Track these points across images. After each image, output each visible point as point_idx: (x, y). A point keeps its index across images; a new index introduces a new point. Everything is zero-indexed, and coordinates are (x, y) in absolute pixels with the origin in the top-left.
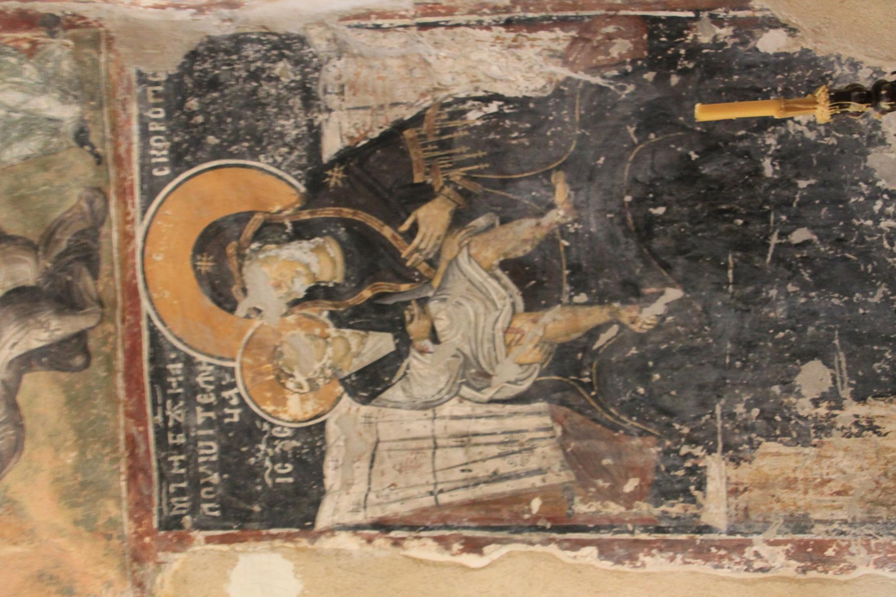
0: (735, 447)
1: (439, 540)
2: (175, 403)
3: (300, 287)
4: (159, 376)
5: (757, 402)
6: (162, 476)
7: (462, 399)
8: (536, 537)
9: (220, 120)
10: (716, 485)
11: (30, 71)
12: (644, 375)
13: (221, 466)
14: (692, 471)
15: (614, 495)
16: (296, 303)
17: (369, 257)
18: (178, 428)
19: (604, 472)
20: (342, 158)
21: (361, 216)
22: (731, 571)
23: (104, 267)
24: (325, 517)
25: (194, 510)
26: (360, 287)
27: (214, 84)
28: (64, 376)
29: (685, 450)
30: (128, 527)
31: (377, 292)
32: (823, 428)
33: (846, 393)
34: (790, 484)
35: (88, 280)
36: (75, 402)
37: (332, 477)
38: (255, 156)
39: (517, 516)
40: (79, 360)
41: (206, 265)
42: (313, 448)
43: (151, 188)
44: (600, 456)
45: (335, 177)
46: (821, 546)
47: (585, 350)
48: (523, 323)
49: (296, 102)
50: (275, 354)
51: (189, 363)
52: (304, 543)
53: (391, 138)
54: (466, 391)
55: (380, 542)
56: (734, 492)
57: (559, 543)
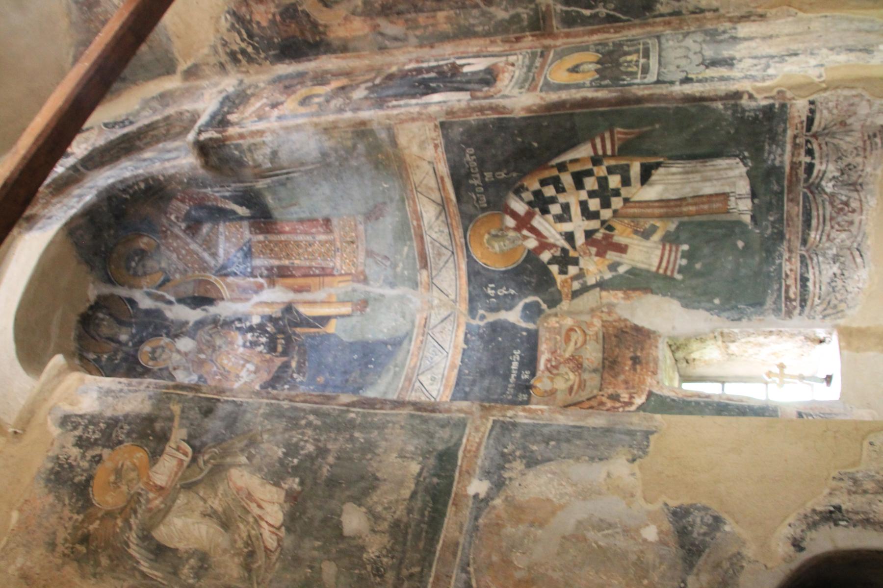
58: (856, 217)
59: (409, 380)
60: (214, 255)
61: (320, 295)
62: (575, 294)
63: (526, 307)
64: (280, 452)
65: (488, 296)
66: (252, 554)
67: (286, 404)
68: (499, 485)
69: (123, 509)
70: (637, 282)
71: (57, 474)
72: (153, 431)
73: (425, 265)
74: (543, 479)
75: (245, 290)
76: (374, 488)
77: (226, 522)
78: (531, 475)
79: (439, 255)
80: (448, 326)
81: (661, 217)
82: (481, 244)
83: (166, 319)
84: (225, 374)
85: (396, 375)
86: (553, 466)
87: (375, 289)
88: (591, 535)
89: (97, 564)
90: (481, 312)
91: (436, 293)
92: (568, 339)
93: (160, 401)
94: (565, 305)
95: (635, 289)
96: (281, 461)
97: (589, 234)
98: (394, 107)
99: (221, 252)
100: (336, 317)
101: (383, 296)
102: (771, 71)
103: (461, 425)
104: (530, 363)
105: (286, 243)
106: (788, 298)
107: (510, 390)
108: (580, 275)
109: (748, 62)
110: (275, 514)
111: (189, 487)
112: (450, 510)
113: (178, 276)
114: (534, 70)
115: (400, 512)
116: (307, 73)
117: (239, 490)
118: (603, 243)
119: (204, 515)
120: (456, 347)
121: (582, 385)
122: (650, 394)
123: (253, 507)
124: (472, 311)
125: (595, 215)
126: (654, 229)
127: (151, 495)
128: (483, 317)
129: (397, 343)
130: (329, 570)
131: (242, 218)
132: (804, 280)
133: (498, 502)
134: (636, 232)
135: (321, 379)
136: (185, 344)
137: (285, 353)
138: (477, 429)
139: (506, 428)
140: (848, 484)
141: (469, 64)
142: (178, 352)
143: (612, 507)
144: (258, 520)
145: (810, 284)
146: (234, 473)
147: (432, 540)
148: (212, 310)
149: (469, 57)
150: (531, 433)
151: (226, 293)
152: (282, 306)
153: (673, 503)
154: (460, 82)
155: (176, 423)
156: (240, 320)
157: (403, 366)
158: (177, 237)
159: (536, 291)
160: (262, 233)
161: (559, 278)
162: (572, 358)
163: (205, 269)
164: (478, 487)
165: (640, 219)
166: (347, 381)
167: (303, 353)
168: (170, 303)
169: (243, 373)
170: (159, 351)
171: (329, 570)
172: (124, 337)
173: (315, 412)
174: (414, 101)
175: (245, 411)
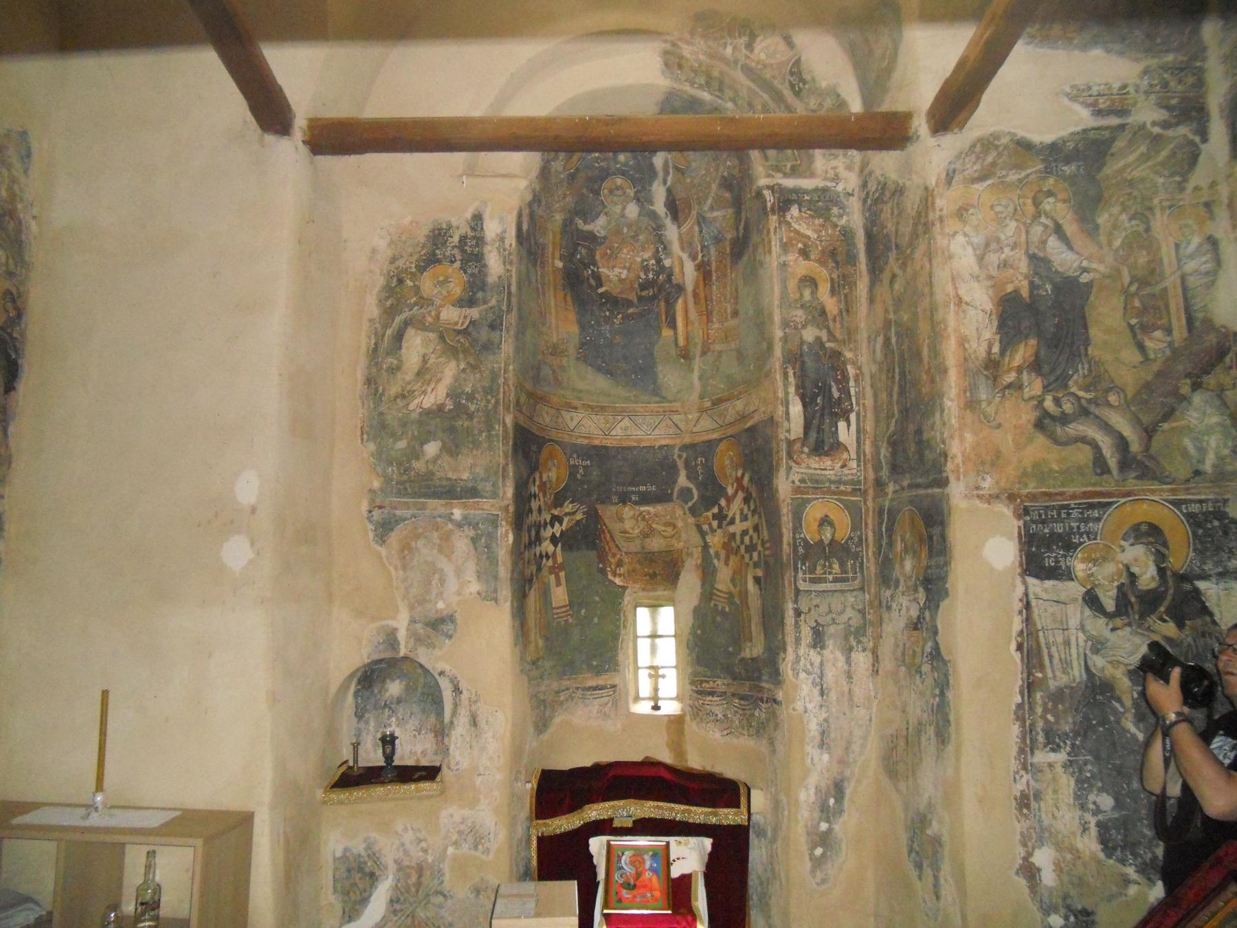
0: (1071, 765)
1: (1022, 631)
2: (1082, 513)
3: (1135, 570)
4: (1091, 506)
5: (1093, 776)
6: (1047, 507)
7: (1086, 642)
8: (1025, 675)
9: (1209, 536)
10: (1053, 757)
11: (1226, 452)
12: (1103, 725)
13: (1052, 534)
14: (1059, 746)
15: (1046, 711)
16: (1127, 568)
17: (1150, 602)
18: (1069, 514)
19: (1055, 706)
20: (1197, 591)
21: (1169, 598)
22: (1014, 765)
23: (1140, 482)
24: (1031, 581)
25: (1033, 521)
26: (1137, 597)
27: (1226, 533)
28: (1091, 464)
29: (1068, 742)
30: (1025, 492)
31: (1133, 604)
32: (1083, 807)
33: (1100, 817)
34: (1055, 792)
35: (1134, 475)
36: (1080, 470)
37: (1049, 583)
38: (1195, 550)
39: (1034, 667)
40: (1099, 471)
41: (1144, 528)
42: (1062, 575)
43: (1177, 504)
44: (1062, 702)
45: (1188, 587)
46: (1028, 806)
47: (1112, 697)
48: (1122, 669)
49: (1221, 570)
50: (1105, 559)
51: (1099, 519)
52: (1019, 570)
53: (1205, 611)
54: (1090, 643)
55: (1020, 604)
56: (1050, 765)
57: (1022, 686)
58: (745, 732)
60: (712, 209)
61: (693, 315)
62: (699, 527)
63: (689, 490)
64: (468, 390)
65: (696, 458)
66: (403, 397)
68: (459, 525)
69: (422, 298)
70: (707, 572)
71: (440, 234)
72: (474, 294)
73: (714, 404)
74: (464, 548)
76: (452, 456)
78: (466, 541)
79: (720, 416)
81: (740, 592)
82: (728, 450)
83: (651, 185)
84: (612, 257)
85: (627, 399)
86: (473, 551)
87: (697, 363)
88: (437, 576)
89: (387, 298)
91: (697, 415)
92: (667, 524)
93: (498, 286)
94: (691, 520)
95: (704, 572)
96: (463, 392)
97: (733, 535)
99: (715, 214)
101: (693, 371)
102: (803, 675)
103: (494, 495)
104: (645, 499)
105: (725, 275)
106: (702, 682)
107: (620, 489)
108: (713, 531)
109: (817, 660)
110: (429, 401)
111: (442, 337)
112: (442, 502)
113: (689, 180)
114: (833, 487)
115: (439, 474)
116: (855, 265)
117: (442, 372)
118: (729, 547)
120: (655, 440)
121: (629, 540)
124: (685, 448)
125: (742, 542)
126: (735, 586)
127: (433, 313)
128: (680, 456)
129: (656, 392)
130: (402, 444)
131: (737, 229)
132: (712, 694)
133: (450, 526)
134: (734, 572)
135: (618, 339)
136: (632, 210)
137: (640, 298)
138: (493, 506)
139: (494, 522)
140: (474, 698)
141: (849, 426)
142: (624, 208)
143: (452, 585)
144: (425, 392)
145: (710, 698)
146: (453, 364)
147: (426, 496)
148: (668, 222)
150: (491, 536)
151: (684, 229)
152: (681, 282)
153: (457, 616)
154: (821, 422)
156: (665, 248)
157: (637, 402)
158: (717, 170)
160: (732, 249)
161: (710, 514)
162: (652, 530)
163: (699, 203)
164: (457, 514)
165: (737, 577)
166: (618, 361)
167: (641, 315)
168: (665, 182)
169: (617, 270)
170: (619, 192)
171: (402, 444)
173: (497, 403)
174: (792, 390)
175: (494, 354)
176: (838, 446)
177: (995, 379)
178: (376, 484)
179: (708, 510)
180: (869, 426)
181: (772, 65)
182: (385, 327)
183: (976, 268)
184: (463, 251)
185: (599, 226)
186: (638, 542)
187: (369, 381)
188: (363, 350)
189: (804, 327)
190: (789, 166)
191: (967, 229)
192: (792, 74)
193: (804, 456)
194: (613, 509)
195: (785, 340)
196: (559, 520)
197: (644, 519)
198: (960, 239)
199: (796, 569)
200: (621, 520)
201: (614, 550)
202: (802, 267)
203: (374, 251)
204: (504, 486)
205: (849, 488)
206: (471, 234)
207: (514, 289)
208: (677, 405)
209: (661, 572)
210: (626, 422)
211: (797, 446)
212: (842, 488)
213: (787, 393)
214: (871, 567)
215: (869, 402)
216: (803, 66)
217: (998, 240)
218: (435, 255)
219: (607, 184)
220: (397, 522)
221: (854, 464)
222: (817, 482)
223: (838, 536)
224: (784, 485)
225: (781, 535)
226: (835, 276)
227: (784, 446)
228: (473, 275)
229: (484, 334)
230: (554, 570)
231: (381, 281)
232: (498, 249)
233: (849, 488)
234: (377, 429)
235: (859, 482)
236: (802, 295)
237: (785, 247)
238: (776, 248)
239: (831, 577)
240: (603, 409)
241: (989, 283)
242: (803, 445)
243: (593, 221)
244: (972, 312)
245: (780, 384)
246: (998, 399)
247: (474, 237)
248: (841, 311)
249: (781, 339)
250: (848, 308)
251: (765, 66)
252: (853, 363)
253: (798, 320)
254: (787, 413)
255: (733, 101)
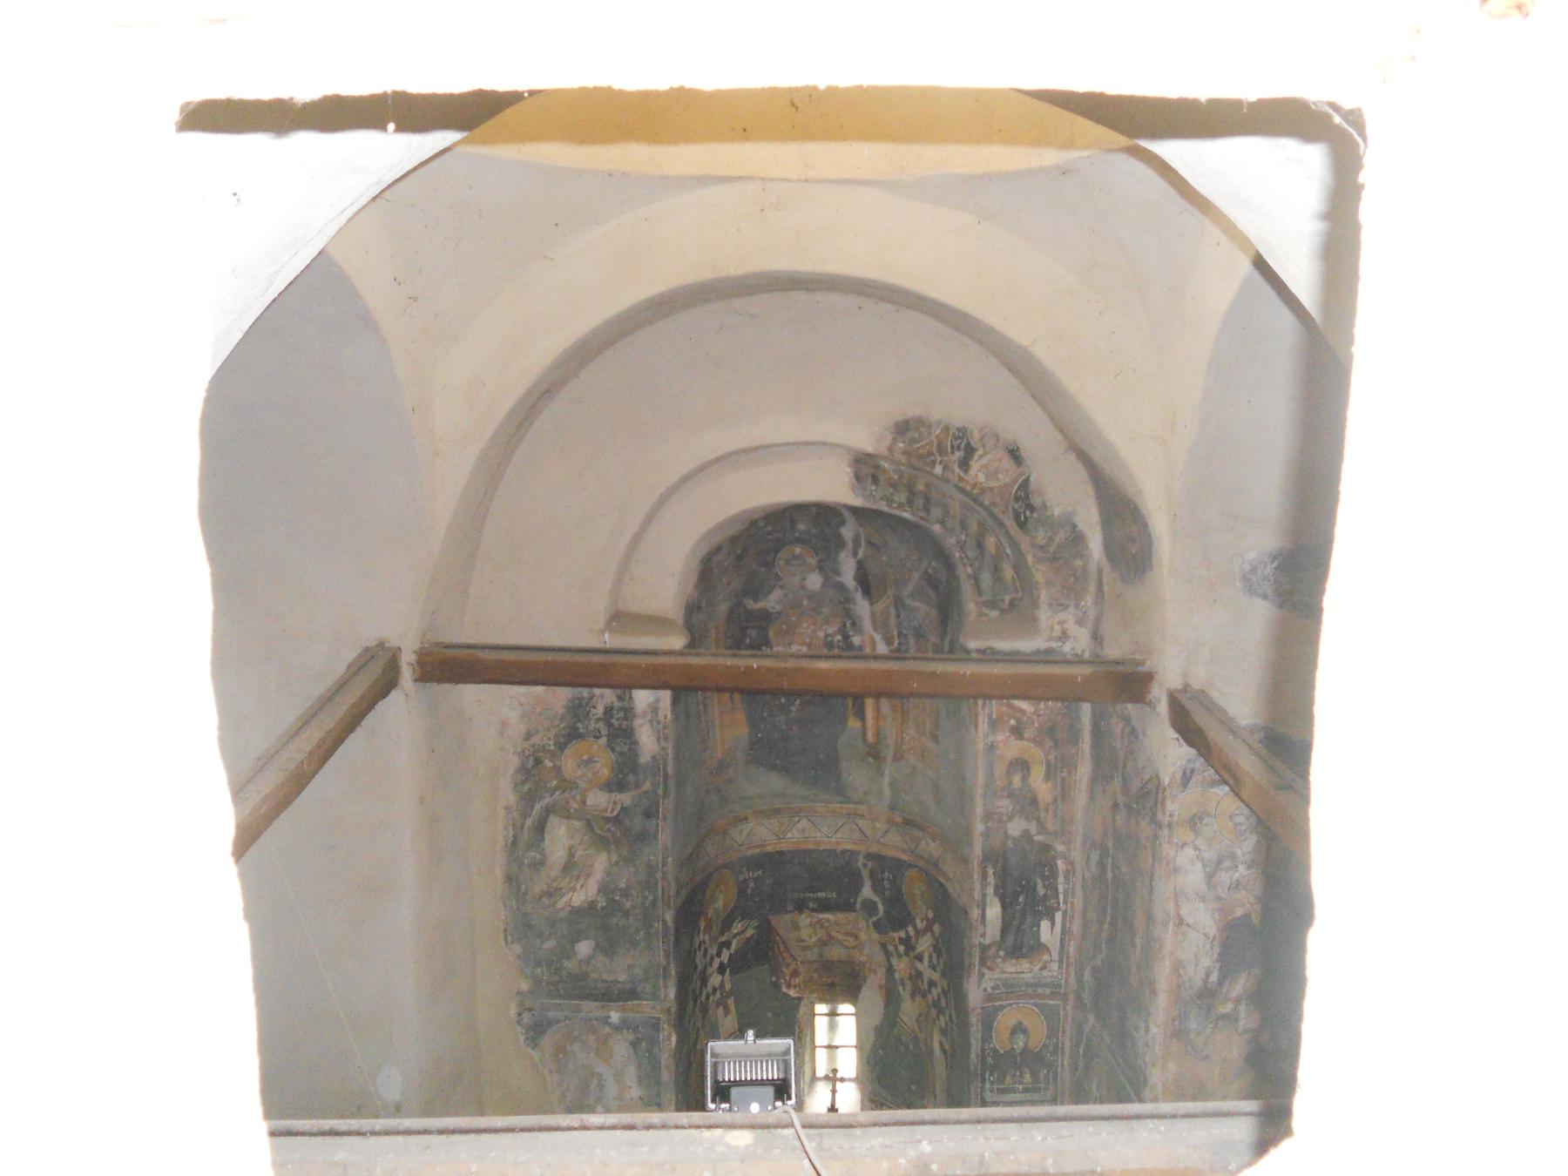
59: (801, 810)
62: (884, 946)
63: (874, 903)
64: (622, 885)
67: (659, 875)
68: (617, 1028)
70: (891, 999)
75: (885, 624)
77: (569, 867)
80: (857, 835)
83: (837, 554)
87: (889, 769)
88: (595, 1081)
89: (524, 782)
90: (870, 864)
92: (847, 934)
94: (875, 936)
98: (984, 875)
100: (864, 726)
103: (655, 997)
104: (825, 906)
110: (578, 899)
111: (589, 824)
115: (593, 976)
119: (570, 848)
121: (806, 948)
122: (800, 999)
123: (582, 881)
124: (869, 856)
128: (865, 866)
129: (840, 791)
130: (550, 944)
136: (814, 581)
139: (655, 1025)
144: (574, 890)
146: (603, 857)
147: (580, 997)
148: (859, 596)
149: (1063, 924)
150: (653, 1042)
151: (881, 605)
154: (1022, 923)
155: (634, 793)
156: (854, 624)
159: (887, 913)
164: (615, 1017)
168: (855, 554)
171: (550, 944)
172: (801, 527)
174: (990, 890)
176: (1039, 947)
177: (1209, 1009)
178: (525, 986)
179: (894, 930)
180: (1076, 928)
181: (991, 489)
182: (524, 816)
183: (1204, 887)
184: (610, 725)
185: (773, 601)
186: (816, 950)
187: (509, 879)
188: (501, 843)
189: (1010, 819)
190: (1007, 599)
191: (1197, 842)
192: (1017, 499)
193: (999, 960)
194: (788, 917)
195: (986, 835)
196: (727, 944)
197: (822, 926)
198: (1190, 852)
199: (983, 1080)
200: (797, 928)
201: (789, 960)
202: (1012, 748)
203: (504, 724)
204: (666, 987)
205: (1048, 991)
206: (617, 704)
207: (670, 770)
208: (863, 808)
209: (841, 982)
210: (804, 823)
211: (992, 951)
212: (1040, 990)
213: (984, 895)
214: (1066, 1076)
215: (1078, 901)
216: (1033, 485)
217: (1233, 857)
218: (576, 729)
219: (783, 555)
220: (550, 1024)
221: (1055, 966)
222: (1012, 986)
223: (1031, 1045)
224: (975, 992)
225: (969, 1044)
226: (1052, 757)
227: (977, 952)
228: (621, 754)
229: (637, 823)
230: (722, 1003)
231: (515, 762)
232: (651, 722)
233: (1048, 991)
234: (522, 929)
235: (1059, 986)
236: (1010, 783)
237: (994, 724)
238: (983, 725)
239: (1021, 1087)
240: (777, 812)
241: (1214, 905)
242: (1000, 948)
243: (766, 596)
244: (1192, 935)
245: (977, 886)
246: (1209, 1030)
247: (621, 709)
248: (1055, 800)
249: (982, 834)
250: (1064, 793)
251: (983, 490)
252: (1066, 858)
253: (1003, 810)
254: (983, 916)
255: (942, 522)
